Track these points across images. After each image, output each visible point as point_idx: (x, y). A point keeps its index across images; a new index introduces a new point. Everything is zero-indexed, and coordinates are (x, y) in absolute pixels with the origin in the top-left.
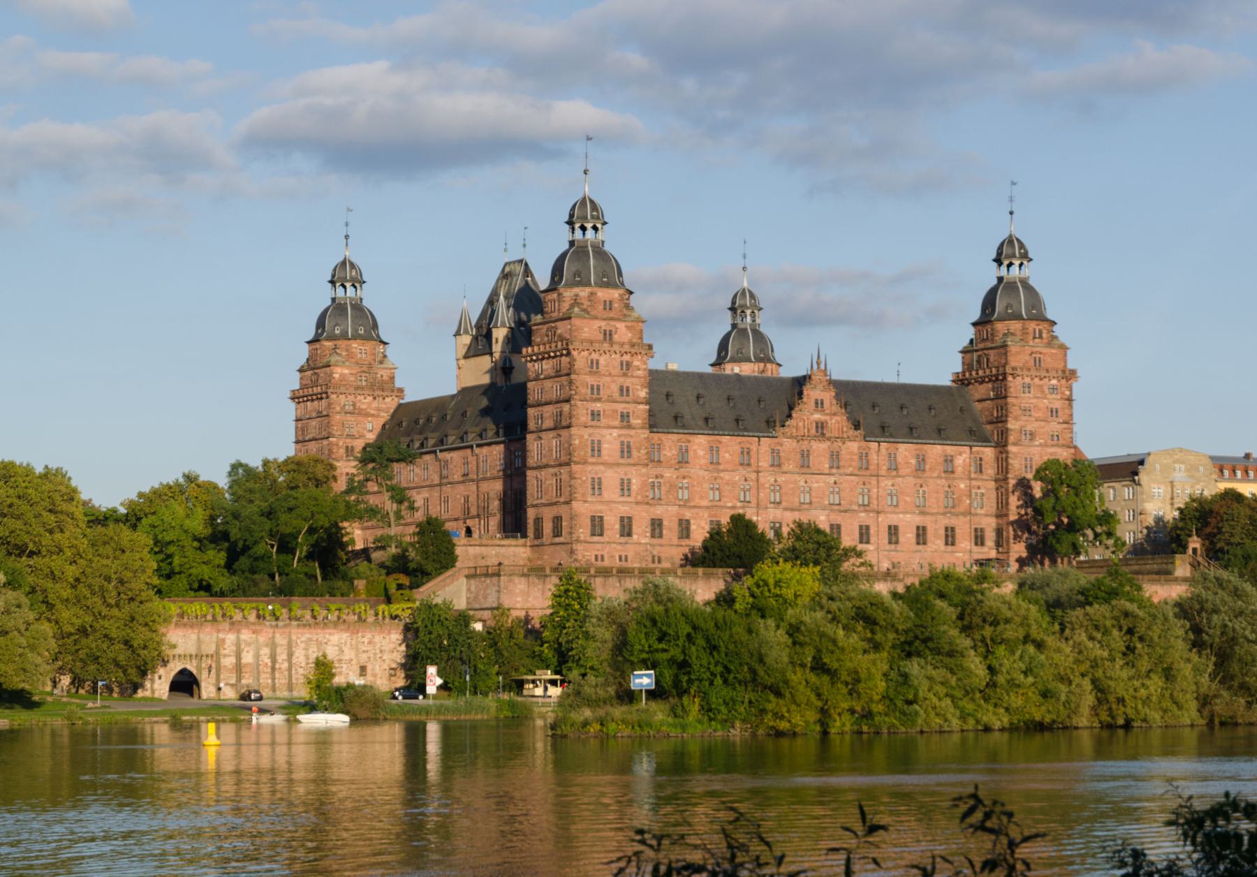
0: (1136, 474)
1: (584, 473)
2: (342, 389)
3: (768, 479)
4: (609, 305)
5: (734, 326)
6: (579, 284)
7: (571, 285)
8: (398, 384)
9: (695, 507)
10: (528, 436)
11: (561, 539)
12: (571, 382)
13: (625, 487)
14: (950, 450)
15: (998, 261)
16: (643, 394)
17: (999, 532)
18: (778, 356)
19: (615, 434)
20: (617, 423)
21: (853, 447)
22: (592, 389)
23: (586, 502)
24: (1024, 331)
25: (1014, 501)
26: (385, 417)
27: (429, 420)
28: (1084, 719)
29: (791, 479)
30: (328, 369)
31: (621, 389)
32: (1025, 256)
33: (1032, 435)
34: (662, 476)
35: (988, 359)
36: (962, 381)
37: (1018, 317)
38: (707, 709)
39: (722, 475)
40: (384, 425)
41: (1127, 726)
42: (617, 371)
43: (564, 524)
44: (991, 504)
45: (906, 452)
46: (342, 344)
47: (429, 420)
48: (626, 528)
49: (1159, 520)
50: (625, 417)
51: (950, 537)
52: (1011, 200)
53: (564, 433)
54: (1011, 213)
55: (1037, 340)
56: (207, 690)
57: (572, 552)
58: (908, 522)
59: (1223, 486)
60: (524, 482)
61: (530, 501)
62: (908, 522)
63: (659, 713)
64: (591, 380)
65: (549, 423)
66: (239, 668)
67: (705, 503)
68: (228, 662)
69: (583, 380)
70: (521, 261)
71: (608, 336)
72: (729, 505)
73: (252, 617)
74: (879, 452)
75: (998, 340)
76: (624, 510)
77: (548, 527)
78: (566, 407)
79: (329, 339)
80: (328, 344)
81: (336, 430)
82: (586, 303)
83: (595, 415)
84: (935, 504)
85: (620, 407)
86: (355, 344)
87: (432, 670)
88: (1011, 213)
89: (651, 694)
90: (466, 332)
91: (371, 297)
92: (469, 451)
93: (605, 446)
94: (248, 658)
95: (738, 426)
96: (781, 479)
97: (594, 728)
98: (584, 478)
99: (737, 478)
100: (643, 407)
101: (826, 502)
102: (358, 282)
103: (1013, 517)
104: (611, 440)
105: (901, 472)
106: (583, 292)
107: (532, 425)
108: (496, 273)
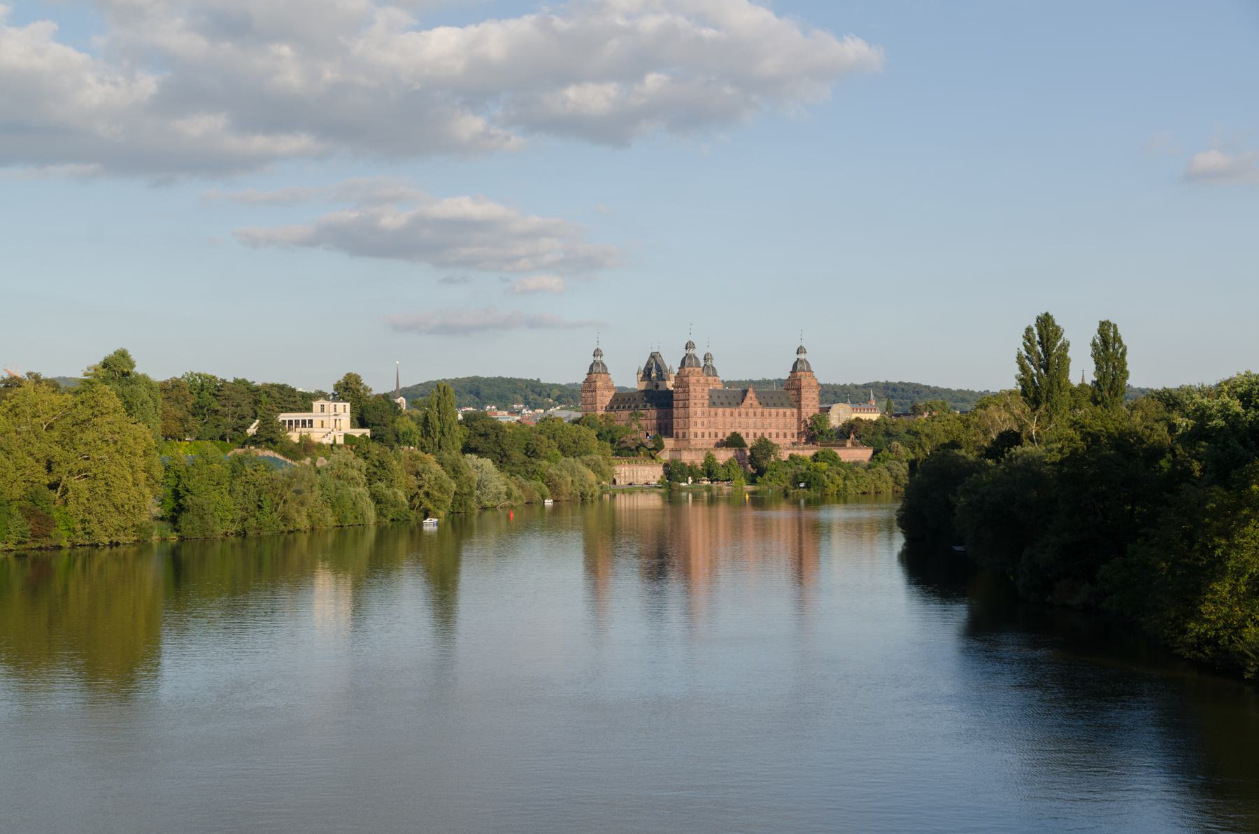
0: (828, 411)
1: (692, 420)
3: (737, 420)
4: (698, 372)
5: (705, 365)
7: (688, 367)
10: (674, 409)
13: (703, 424)
14: (785, 410)
15: (798, 353)
16: (707, 397)
17: (798, 434)
18: (718, 375)
20: (701, 406)
21: (760, 410)
24: (806, 375)
25: (803, 426)
26: (611, 397)
27: (629, 399)
28: (872, 492)
29: (743, 420)
32: (805, 352)
33: (808, 405)
37: (804, 371)
38: (814, 490)
40: (611, 400)
41: (880, 492)
44: (796, 426)
45: (773, 411)
46: (599, 375)
47: (629, 399)
48: (703, 436)
49: (834, 427)
51: (785, 436)
56: (618, 481)
57: (689, 442)
58: (774, 431)
59: (854, 416)
61: (674, 427)
62: (774, 431)
63: (805, 490)
64: (694, 394)
65: (681, 405)
66: (625, 477)
68: (623, 475)
69: (692, 394)
70: (658, 353)
71: (698, 381)
73: (627, 463)
74: (766, 411)
75: (798, 377)
76: (702, 430)
77: (681, 435)
78: (687, 402)
79: (595, 373)
80: (594, 375)
81: (598, 401)
83: (695, 404)
84: (781, 426)
85: (701, 401)
86: (603, 375)
87: (690, 478)
89: (803, 488)
91: (605, 360)
92: (647, 411)
94: (627, 474)
95: (730, 405)
97: (796, 494)
102: (601, 355)
103: (802, 430)
104: (699, 410)
105: (773, 417)
106: (692, 369)
107: (675, 406)
108: (649, 355)
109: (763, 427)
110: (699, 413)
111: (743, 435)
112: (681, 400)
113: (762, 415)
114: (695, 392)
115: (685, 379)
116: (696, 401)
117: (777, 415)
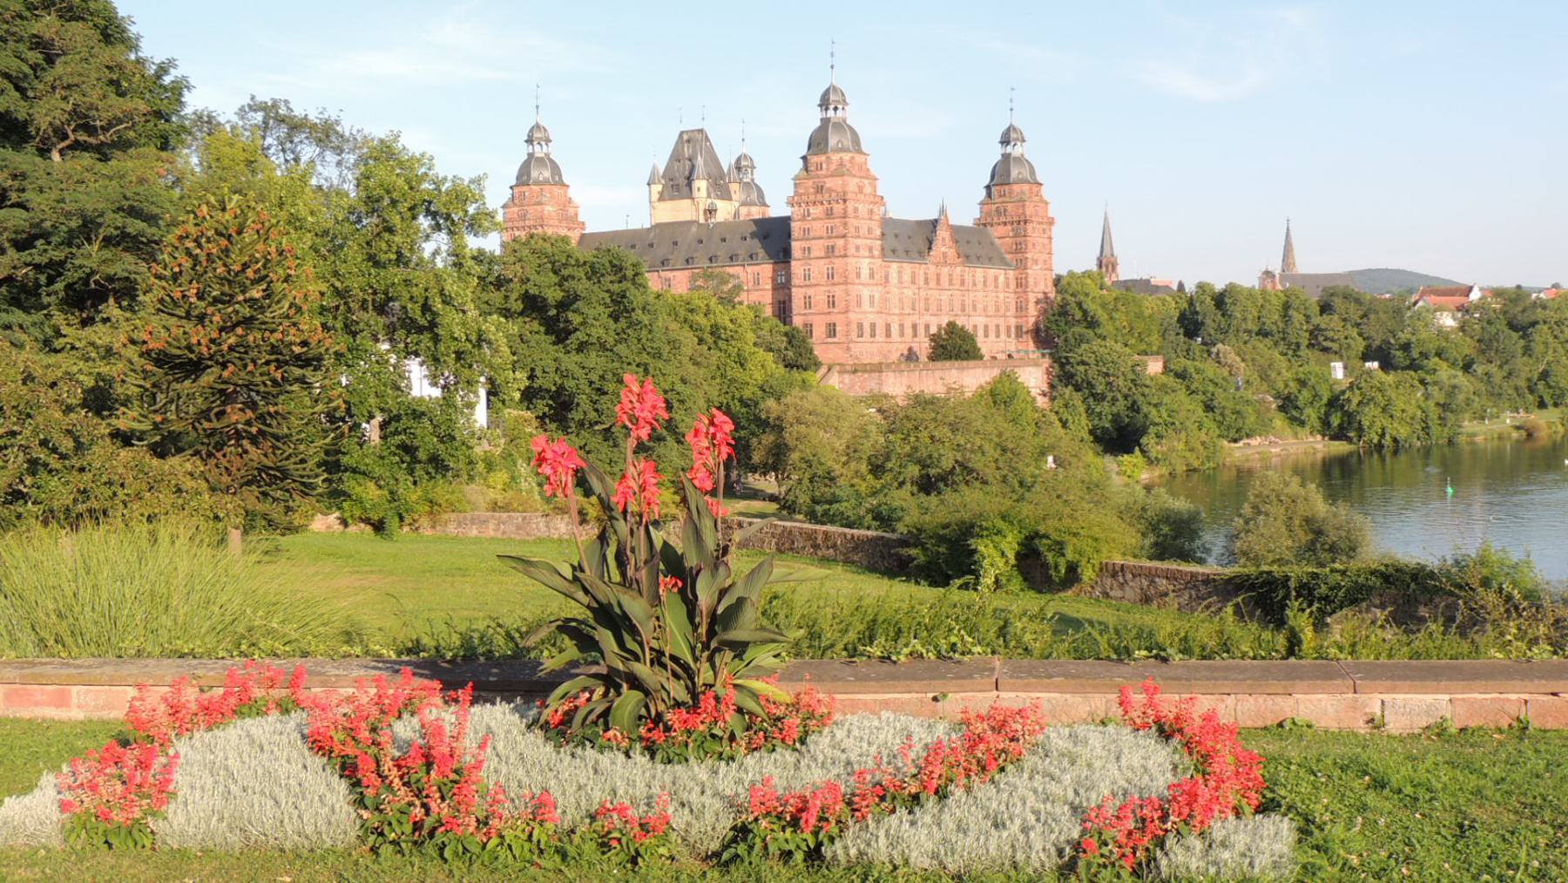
2: (551, 222)
6: (842, 150)
8: (581, 219)
10: (793, 263)
11: (835, 340)
12: (845, 224)
16: (878, 232)
20: (867, 254)
30: (539, 208)
32: (1023, 141)
35: (1005, 211)
36: (983, 224)
42: (866, 216)
43: (838, 328)
45: (979, 273)
50: (871, 249)
52: (1011, 101)
53: (838, 262)
57: (848, 349)
60: (790, 296)
67: (897, 311)
69: (852, 222)
70: (701, 131)
76: (871, 317)
78: (840, 242)
79: (537, 183)
82: (848, 165)
85: (869, 242)
86: (555, 189)
90: (660, 182)
91: (556, 152)
96: (930, 292)
100: (879, 242)
102: (548, 141)
104: (865, 264)
106: (846, 157)
109: (963, 310)
110: (865, 272)
111: (971, 330)
112: (821, 238)
113: (963, 283)
114: (856, 217)
115: (830, 183)
116: (858, 241)
117: (985, 282)
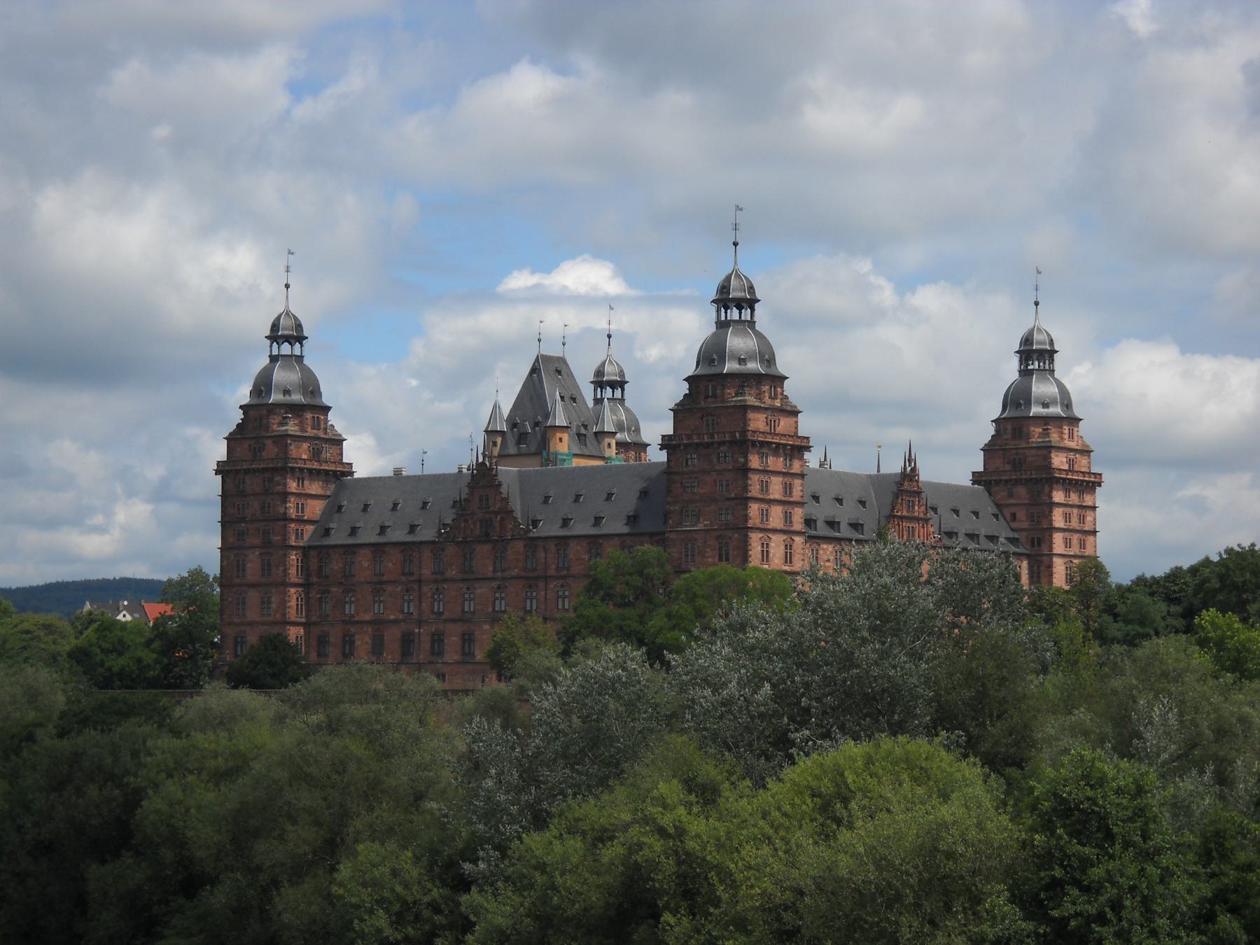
9: (357, 622)
19: (257, 553)
20: (257, 541)
22: (238, 509)
23: (230, 624)
31: (263, 507)
34: (329, 592)
39: (384, 586)
54: (735, 244)
55: (709, 400)
67: (367, 617)
72: (392, 617)
88: (735, 244)
93: (249, 565)
98: (230, 599)
99: (400, 588)
101: (490, 610)
